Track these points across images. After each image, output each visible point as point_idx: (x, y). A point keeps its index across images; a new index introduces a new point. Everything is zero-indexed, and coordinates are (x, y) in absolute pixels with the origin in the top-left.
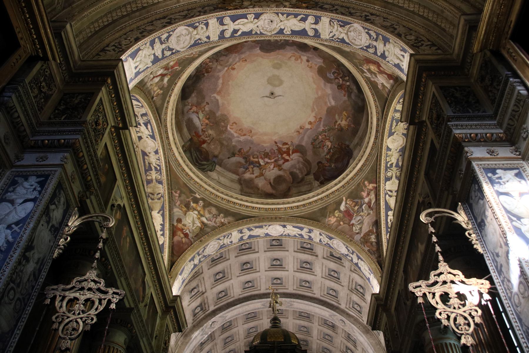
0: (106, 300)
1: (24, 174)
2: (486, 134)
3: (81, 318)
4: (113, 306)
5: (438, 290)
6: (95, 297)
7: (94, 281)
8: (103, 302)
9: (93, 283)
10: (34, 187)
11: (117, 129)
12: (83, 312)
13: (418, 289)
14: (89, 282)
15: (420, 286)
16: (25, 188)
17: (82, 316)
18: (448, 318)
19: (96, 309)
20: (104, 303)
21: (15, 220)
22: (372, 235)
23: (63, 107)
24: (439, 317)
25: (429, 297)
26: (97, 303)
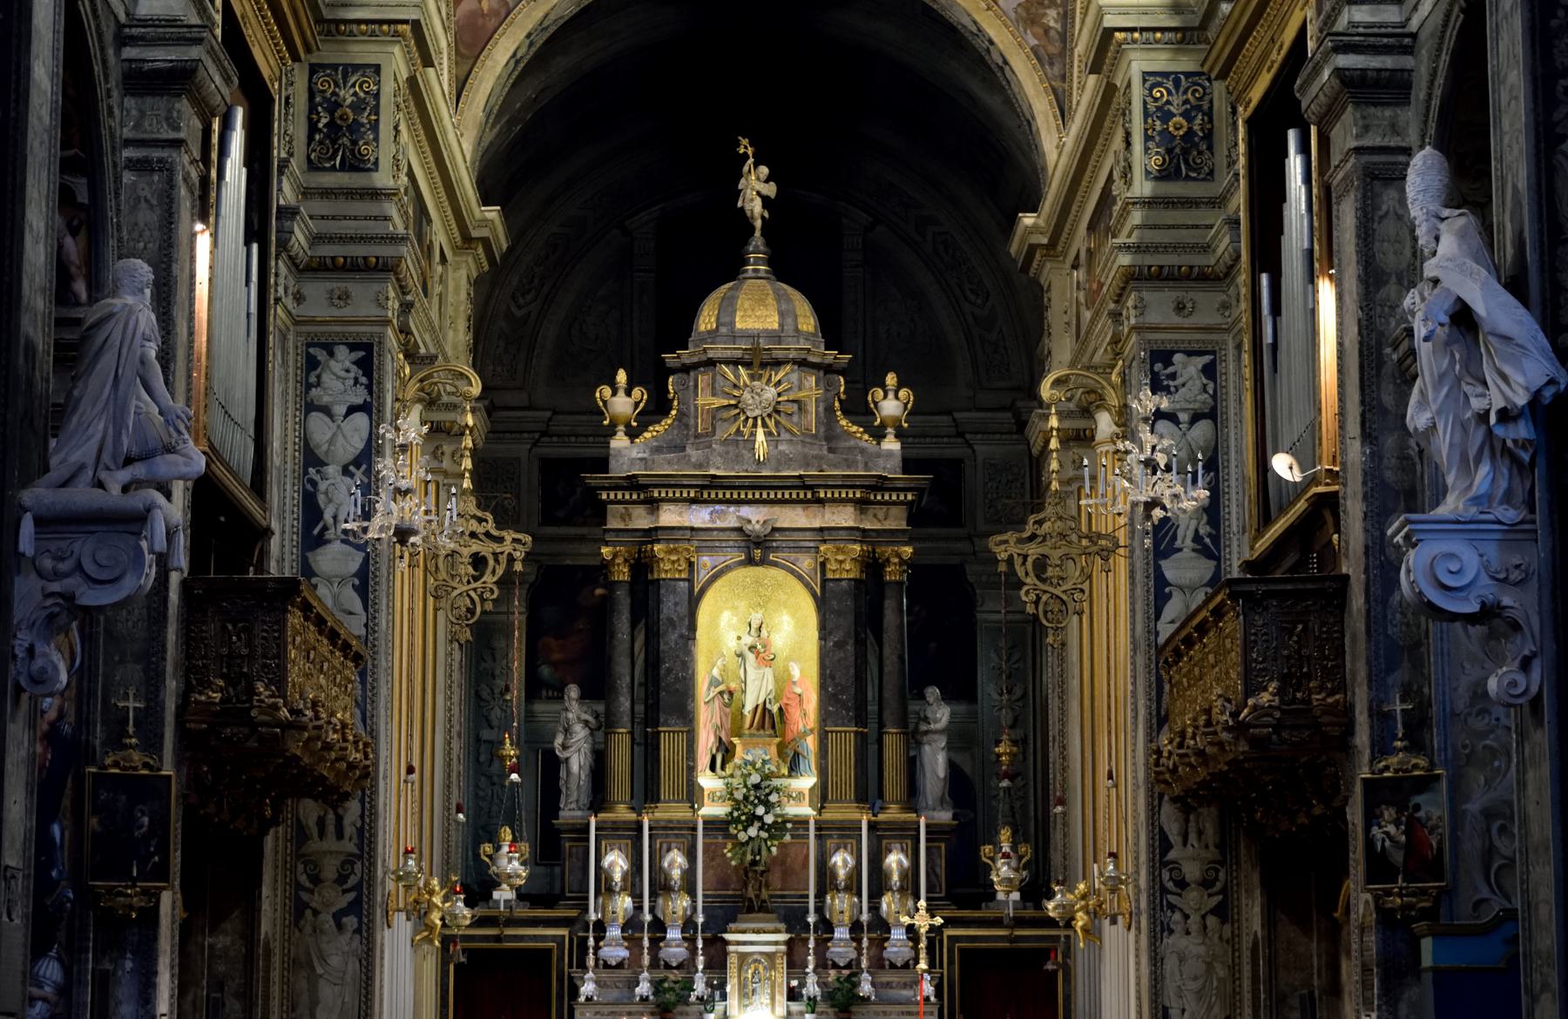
0: (505, 555)
1: (323, 340)
2: (1180, 267)
3: (475, 590)
4: (518, 567)
5: (1033, 551)
6: (486, 548)
7: (474, 517)
8: (500, 557)
9: (473, 522)
10: (352, 375)
11: (412, 82)
12: (476, 579)
13: (1003, 547)
14: (467, 521)
15: (1006, 542)
16: (338, 377)
17: (474, 585)
18: (1036, 603)
19: (494, 572)
20: (503, 559)
21: (350, 457)
22: (1049, 7)
23: (324, 121)
24: (1024, 598)
25: (1018, 561)
26: (491, 562)
